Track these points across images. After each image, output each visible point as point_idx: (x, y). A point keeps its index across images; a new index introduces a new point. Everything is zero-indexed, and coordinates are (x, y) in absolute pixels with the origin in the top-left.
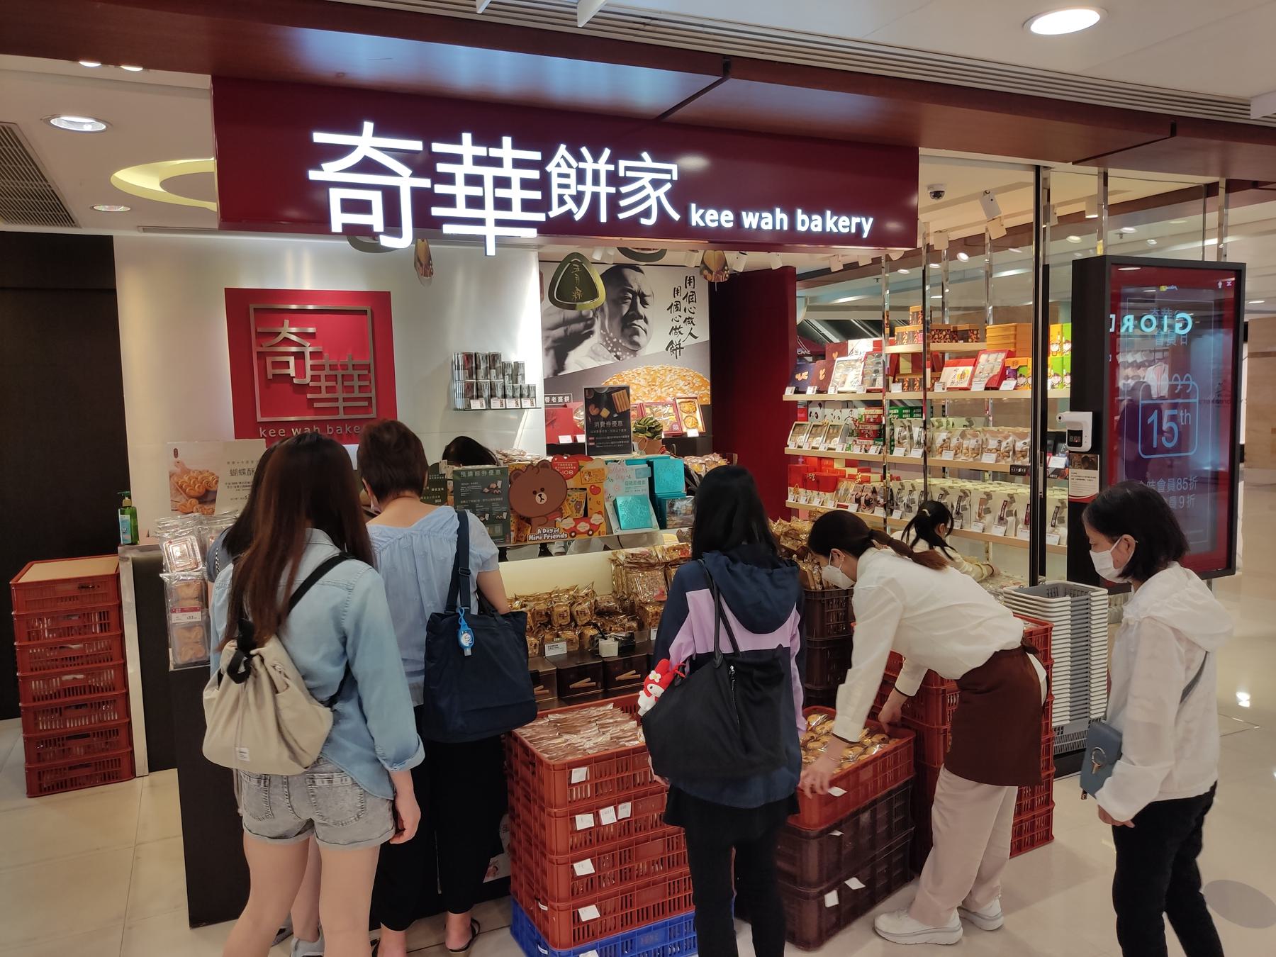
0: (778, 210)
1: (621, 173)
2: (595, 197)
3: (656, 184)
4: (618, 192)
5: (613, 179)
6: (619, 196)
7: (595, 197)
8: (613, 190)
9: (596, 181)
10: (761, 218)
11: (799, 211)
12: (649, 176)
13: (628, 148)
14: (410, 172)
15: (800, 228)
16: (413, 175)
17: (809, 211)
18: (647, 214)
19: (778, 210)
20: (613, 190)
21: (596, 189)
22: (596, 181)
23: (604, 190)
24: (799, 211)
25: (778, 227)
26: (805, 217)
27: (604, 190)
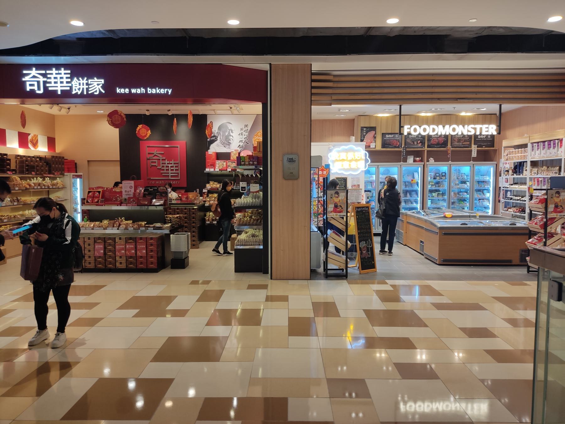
0: (142, 88)
1: (89, 83)
2: (83, 89)
3: (98, 85)
4: (89, 87)
5: (87, 84)
6: (89, 88)
7: (83, 89)
8: (87, 87)
9: (83, 85)
10: (137, 90)
11: (148, 88)
12: (95, 84)
13: (90, 77)
14: (42, 77)
15: (149, 92)
16: (43, 78)
17: (152, 88)
18: (96, 91)
19: (142, 88)
20: (87, 87)
21: (83, 87)
22: (83, 85)
23: (85, 87)
24: (148, 88)
25: (142, 92)
26: (150, 90)
27: (85, 87)
